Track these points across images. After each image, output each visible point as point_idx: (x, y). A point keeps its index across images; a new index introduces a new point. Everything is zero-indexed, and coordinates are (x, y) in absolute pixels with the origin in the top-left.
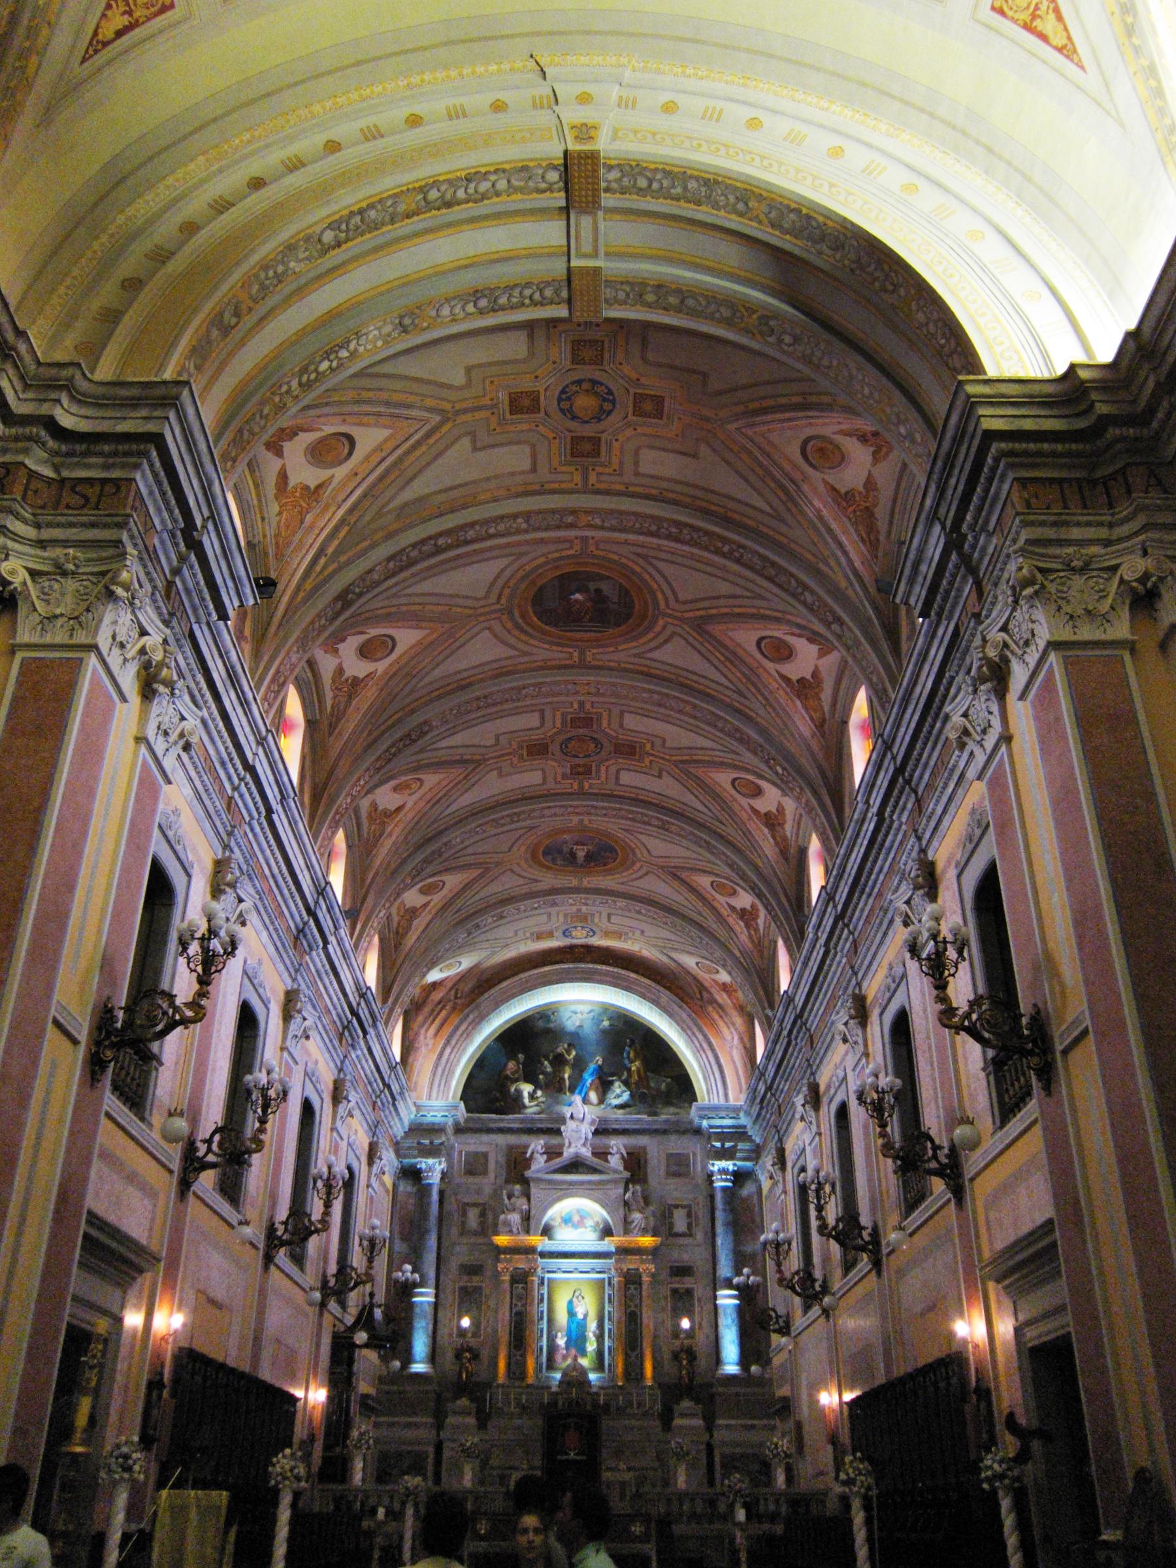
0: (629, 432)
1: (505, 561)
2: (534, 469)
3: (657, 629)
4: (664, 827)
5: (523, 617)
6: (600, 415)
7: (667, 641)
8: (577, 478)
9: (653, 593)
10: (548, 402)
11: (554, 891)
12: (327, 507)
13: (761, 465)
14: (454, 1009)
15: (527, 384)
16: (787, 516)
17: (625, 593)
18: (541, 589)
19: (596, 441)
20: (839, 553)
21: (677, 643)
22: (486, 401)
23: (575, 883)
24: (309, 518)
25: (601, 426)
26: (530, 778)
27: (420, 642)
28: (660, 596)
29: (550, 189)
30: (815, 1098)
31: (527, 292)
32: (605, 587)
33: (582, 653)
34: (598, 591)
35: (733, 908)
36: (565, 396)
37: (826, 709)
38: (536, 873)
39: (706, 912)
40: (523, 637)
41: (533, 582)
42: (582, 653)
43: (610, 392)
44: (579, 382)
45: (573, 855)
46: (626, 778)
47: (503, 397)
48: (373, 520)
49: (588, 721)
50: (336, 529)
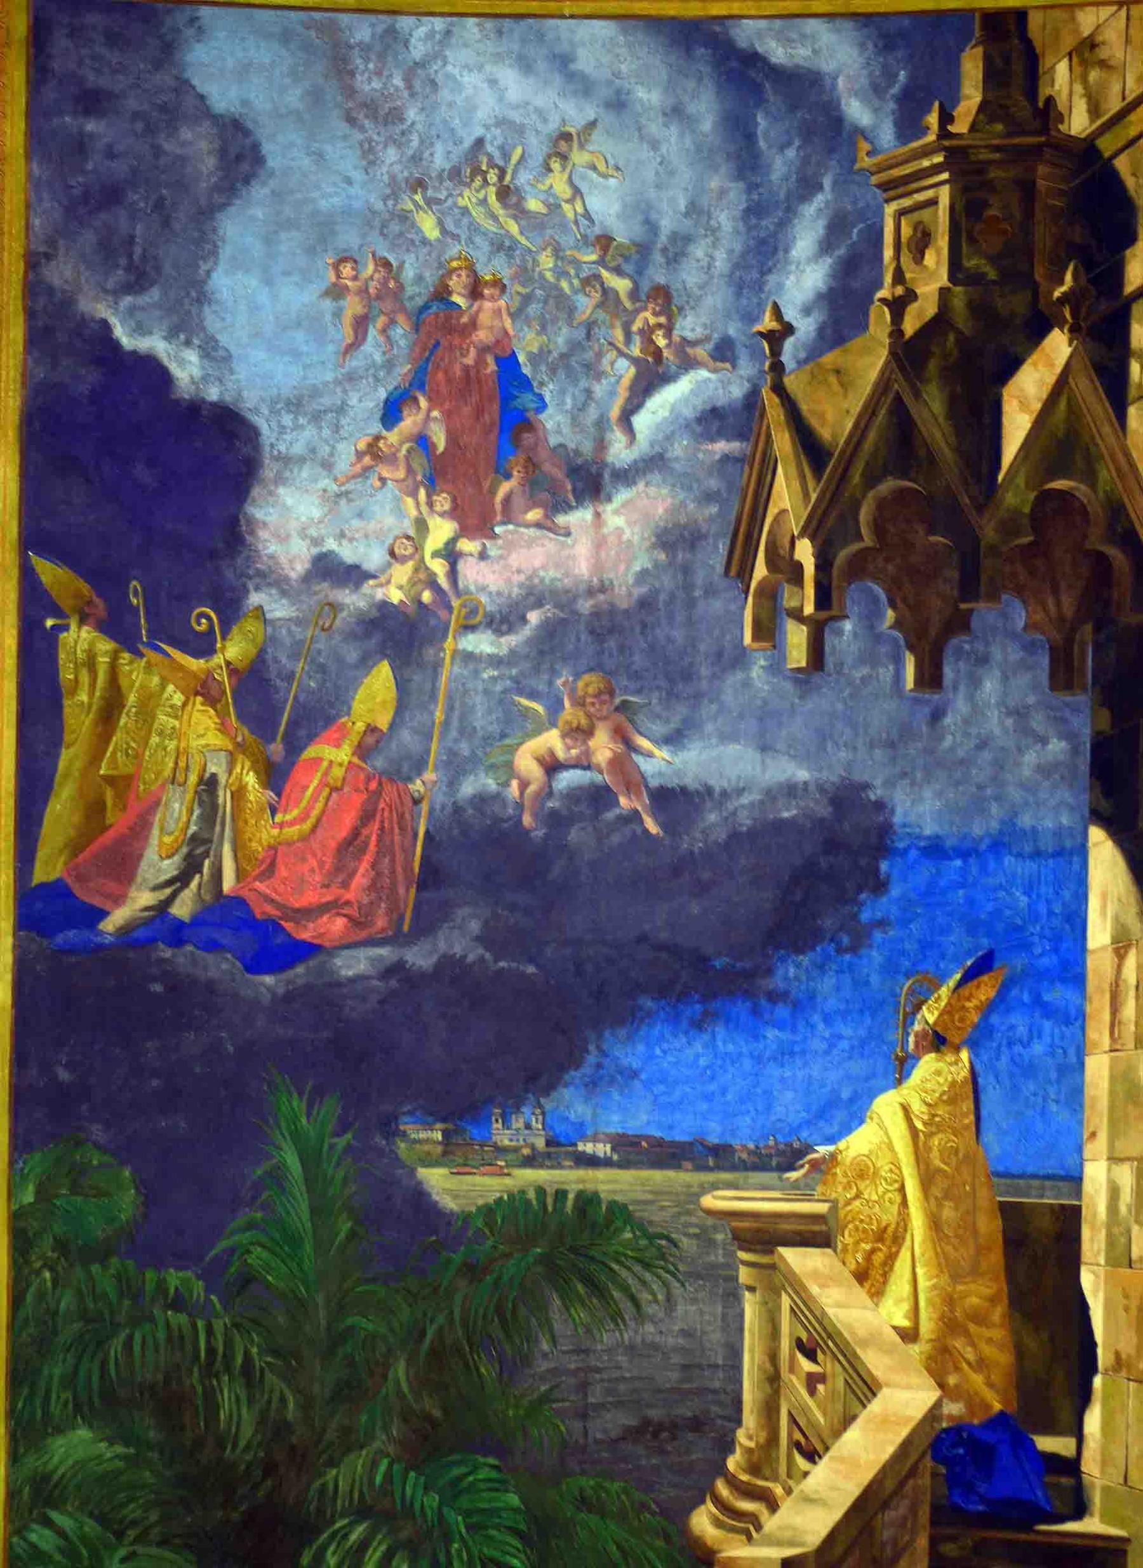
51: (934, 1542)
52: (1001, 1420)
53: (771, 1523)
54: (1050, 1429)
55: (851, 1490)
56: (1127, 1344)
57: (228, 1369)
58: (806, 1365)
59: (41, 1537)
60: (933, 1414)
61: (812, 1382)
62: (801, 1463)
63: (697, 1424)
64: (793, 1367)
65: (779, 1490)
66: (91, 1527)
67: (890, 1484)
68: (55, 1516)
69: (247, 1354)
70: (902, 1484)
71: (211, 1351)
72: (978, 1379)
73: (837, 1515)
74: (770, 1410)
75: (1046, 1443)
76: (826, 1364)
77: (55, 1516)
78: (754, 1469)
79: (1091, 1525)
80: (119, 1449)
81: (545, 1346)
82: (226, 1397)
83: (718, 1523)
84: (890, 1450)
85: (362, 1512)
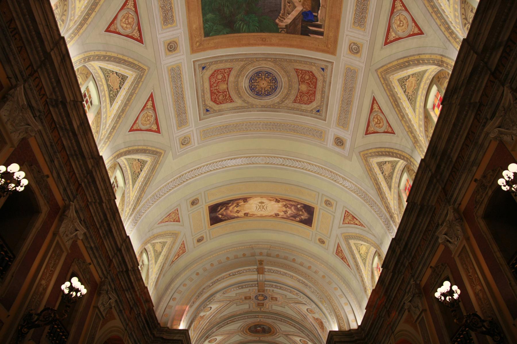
0: (270, 303)
1: (242, 323)
2: (249, 308)
3: (277, 335)
5: (246, 332)
6: (264, 300)
7: (279, 337)
8: (259, 309)
10: (253, 297)
12: (205, 319)
13: (298, 311)
15: (248, 295)
16: (305, 321)
17: (269, 329)
18: (250, 327)
19: (263, 304)
20: (316, 330)
21: (281, 338)
22: (240, 298)
24: (201, 322)
25: (264, 301)
27: (222, 338)
28: (277, 329)
29: (254, 271)
31: (249, 285)
32: (265, 327)
33: (260, 338)
34: (263, 327)
36: (256, 297)
40: (246, 335)
41: (248, 326)
42: (260, 338)
43: (266, 296)
44: (260, 295)
47: (243, 297)
48: (214, 320)
50: (207, 324)
51: (302, 23)
52: (309, 11)
53: (284, 21)
54: (315, 13)
55: (293, 18)
56: (324, 4)
57: (225, 6)
58: (289, 4)
59: (207, 25)
60: (302, 10)
61: (289, 6)
62: (288, 15)
63: (276, 11)
64: (287, 4)
65: (285, 18)
66: (212, 24)
67: (297, 17)
68: (208, 23)
69: (227, 5)
70: (298, 17)
71: (223, 4)
72: (307, 7)
73: (292, 20)
74: (284, 9)
75: (314, 14)
76: (291, 4)
77: (208, 23)
78: (283, 15)
79: (318, 23)
80: (214, 16)
81: (260, 2)
82: (225, 9)
83: (279, 21)
84: (297, 14)
85: (241, 20)
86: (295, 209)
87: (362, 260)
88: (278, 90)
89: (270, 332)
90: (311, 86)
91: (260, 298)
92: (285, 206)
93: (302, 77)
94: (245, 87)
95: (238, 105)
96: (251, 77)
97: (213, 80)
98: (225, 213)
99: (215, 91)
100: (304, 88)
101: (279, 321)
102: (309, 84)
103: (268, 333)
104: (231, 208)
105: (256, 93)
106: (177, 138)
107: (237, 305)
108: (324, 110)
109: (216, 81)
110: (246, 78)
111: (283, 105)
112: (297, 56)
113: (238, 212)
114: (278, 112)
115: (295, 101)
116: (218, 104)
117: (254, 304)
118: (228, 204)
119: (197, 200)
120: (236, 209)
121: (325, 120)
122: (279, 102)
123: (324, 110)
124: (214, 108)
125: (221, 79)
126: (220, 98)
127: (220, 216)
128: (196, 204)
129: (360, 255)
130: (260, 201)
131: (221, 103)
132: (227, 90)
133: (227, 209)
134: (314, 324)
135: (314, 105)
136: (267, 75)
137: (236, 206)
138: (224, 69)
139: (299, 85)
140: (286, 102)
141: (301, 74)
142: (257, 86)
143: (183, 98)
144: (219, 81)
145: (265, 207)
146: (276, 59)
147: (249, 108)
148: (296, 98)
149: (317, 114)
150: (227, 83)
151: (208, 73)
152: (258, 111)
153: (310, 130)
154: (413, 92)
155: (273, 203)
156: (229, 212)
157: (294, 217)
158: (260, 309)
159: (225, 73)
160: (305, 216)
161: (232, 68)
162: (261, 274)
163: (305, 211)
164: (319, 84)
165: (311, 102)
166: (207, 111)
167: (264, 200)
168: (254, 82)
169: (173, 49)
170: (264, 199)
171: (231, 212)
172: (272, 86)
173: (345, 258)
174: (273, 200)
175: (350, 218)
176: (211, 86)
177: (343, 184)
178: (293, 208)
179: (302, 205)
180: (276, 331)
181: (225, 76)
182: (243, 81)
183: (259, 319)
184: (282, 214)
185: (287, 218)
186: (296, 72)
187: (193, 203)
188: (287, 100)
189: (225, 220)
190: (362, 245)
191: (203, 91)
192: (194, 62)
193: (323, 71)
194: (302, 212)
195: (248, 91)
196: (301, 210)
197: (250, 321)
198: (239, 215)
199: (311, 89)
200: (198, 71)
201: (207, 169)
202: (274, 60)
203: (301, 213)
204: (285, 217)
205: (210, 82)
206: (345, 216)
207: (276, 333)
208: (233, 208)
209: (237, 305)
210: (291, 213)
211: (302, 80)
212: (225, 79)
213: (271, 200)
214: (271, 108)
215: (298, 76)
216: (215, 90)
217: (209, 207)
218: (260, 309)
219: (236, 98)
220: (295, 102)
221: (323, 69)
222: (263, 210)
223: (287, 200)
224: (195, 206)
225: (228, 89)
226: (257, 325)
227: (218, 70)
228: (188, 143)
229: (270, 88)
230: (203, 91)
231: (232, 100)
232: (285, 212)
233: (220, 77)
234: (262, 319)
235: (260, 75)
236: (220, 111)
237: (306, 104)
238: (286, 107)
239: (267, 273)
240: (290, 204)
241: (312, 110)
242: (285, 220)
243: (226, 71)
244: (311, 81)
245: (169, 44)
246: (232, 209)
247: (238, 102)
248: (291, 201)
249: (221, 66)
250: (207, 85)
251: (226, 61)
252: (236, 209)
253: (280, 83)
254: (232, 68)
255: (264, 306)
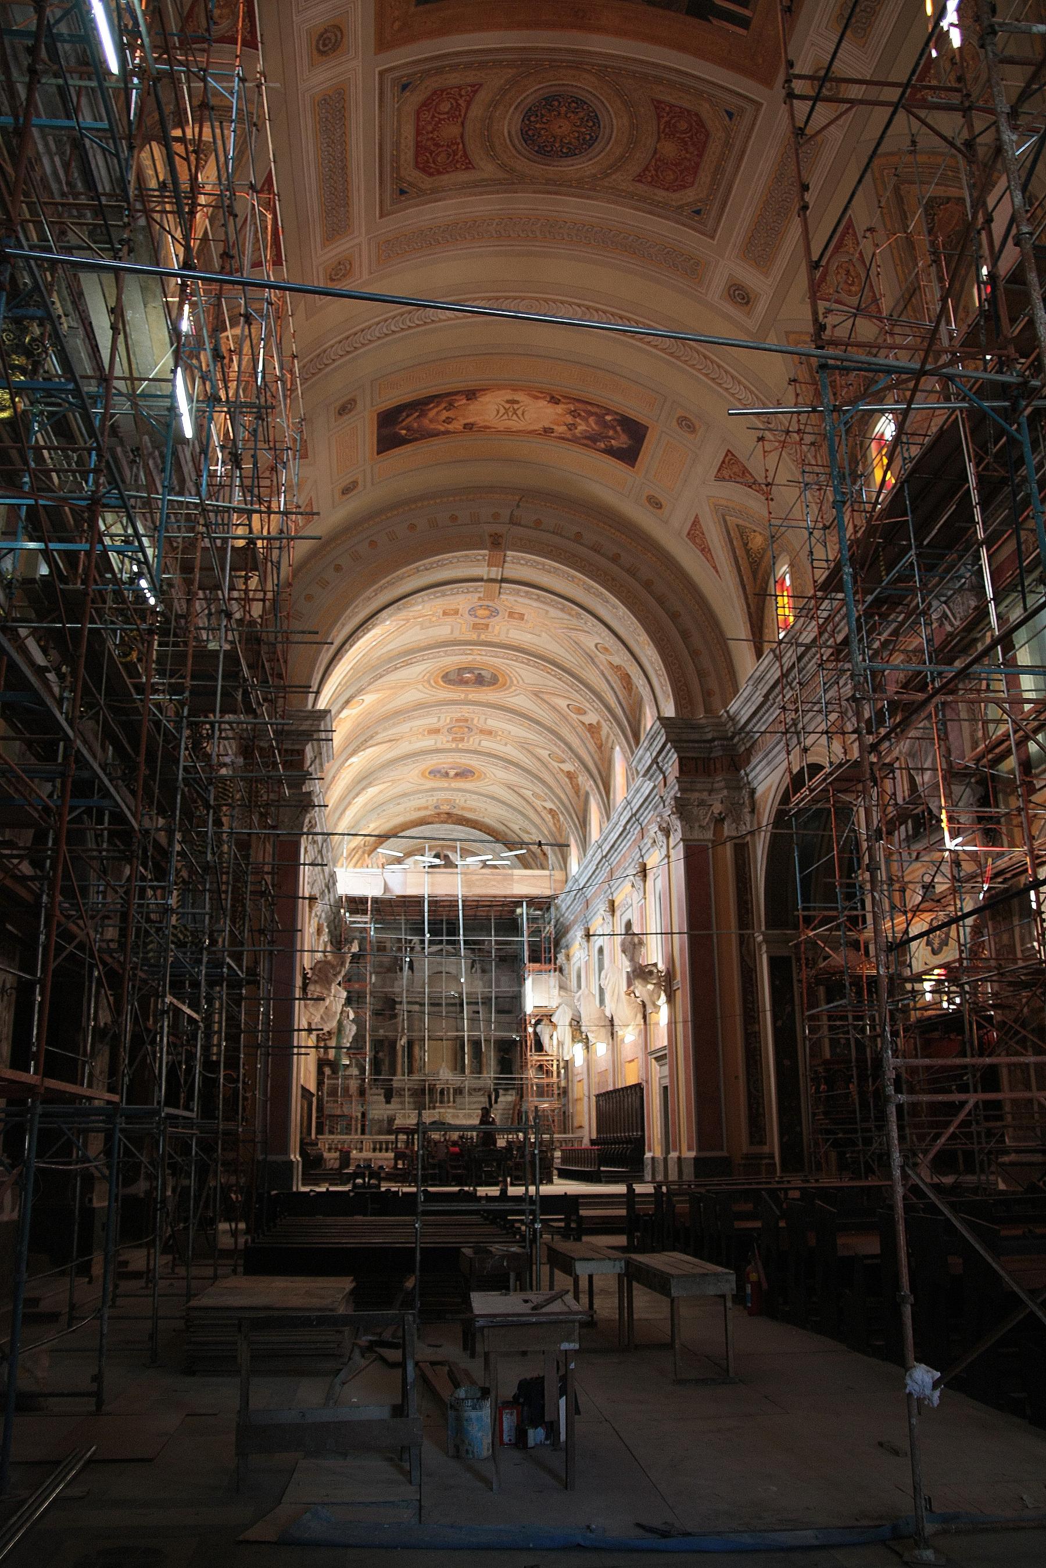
4: (506, 768)
9: (510, 678)
11: (433, 789)
14: (364, 853)
19: (487, 625)
23: (446, 785)
26: (429, 742)
30: (588, 936)
32: (483, 672)
35: (545, 808)
37: (604, 739)
38: (422, 781)
39: (528, 807)
45: (447, 774)
46: (484, 743)
49: (466, 720)
86: (596, 423)
87: (751, 563)
88: (597, 147)
89: (494, 684)
90: (691, 149)
91: (480, 612)
92: (574, 413)
93: (668, 123)
94: (509, 132)
95: (486, 176)
96: (530, 109)
97: (426, 116)
98: (415, 425)
99: (429, 143)
100: (669, 149)
101: (523, 662)
102: (686, 143)
103: (488, 686)
104: (432, 414)
105: (536, 148)
106: (321, 269)
107: (422, 629)
108: (713, 213)
109: (433, 117)
110: (516, 108)
111: (606, 184)
112: (665, 67)
113: (448, 420)
114: (588, 198)
115: (639, 179)
116: (431, 175)
117: (464, 626)
118: (427, 404)
119: (353, 401)
120: (445, 414)
121: (713, 238)
122: (595, 175)
123: (713, 213)
124: (421, 185)
125: (447, 113)
126: (439, 159)
127: (404, 432)
128: (350, 411)
129: (748, 551)
130: (510, 398)
131: (439, 173)
132: (459, 140)
133: (423, 414)
134: (610, 678)
135: (690, 195)
136: (574, 105)
137: (445, 408)
138: (460, 88)
139: (659, 140)
140: (614, 177)
141: (668, 114)
142: (542, 132)
143: (344, 168)
144: (442, 117)
145: (519, 412)
146: (606, 67)
147: (513, 183)
148: (644, 171)
149: (693, 219)
150: (463, 124)
151: (415, 99)
152: (534, 192)
153: (668, 252)
154: (949, 237)
155: (542, 403)
156: (426, 422)
157: (590, 440)
158: (479, 636)
159: (461, 96)
160: (622, 441)
161: (481, 85)
162: (495, 566)
163: (623, 430)
164: (714, 149)
165: (685, 187)
166: (402, 192)
167: (520, 396)
168: (537, 122)
169: (330, 46)
170: (520, 393)
171: (431, 421)
172: (583, 133)
173: (709, 550)
174: (544, 398)
175: (735, 469)
176: (418, 133)
177: (732, 391)
178: (592, 420)
179: (618, 417)
180: (512, 682)
181: (458, 105)
182: (508, 117)
183: (470, 658)
184: (562, 429)
185: (575, 440)
186: (656, 108)
187: (344, 410)
188: (619, 174)
189: (416, 440)
190: (755, 531)
191: (397, 145)
192: (381, 74)
193: (731, 119)
194: (616, 432)
195: (516, 142)
196: (614, 428)
197: (452, 660)
198: (450, 427)
199: (688, 156)
200: (388, 94)
201: (385, 330)
202: (600, 71)
203: (611, 433)
204: (570, 437)
205: (418, 119)
206: (723, 462)
207: (510, 687)
208: (438, 413)
209: (422, 629)
210: (586, 431)
211: (667, 130)
212: (457, 113)
213: (537, 398)
214: (571, 186)
215: (659, 117)
216: (428, 140)
217: (378, 414)
218: (479, 636)
219: (482, 159)
220: (639, 181)
221: (730, 115)
222: (515, 417)
223: (579, 401)
224: (346, 417)
225: (462, 137)
226: (465, 668)
227: (442, 91)
228: (344, 276)
229: (578, 138)
230: (397, 145)
231: (470, 163)
232: (571, 427)
233: (445, 107)
234: (478, 658)
235: (556, 103)
236: (434, 191)
237: (667, 189)
238: (612, 188)
239: (512, 566)
240: (584, 411)
241: (681, 207)
242: (566, 445)
243: (463, 93)
244: (691, 138)
245: (321, 35)
246: (435, 417)
247: (488, 169)
248: (590, 404)
249: (453, 79)
250: (409, 131)
251: (468, 66)
252: (445, 414)
253: (608, 131)
254: (481, 85)
255: (490, 629)
